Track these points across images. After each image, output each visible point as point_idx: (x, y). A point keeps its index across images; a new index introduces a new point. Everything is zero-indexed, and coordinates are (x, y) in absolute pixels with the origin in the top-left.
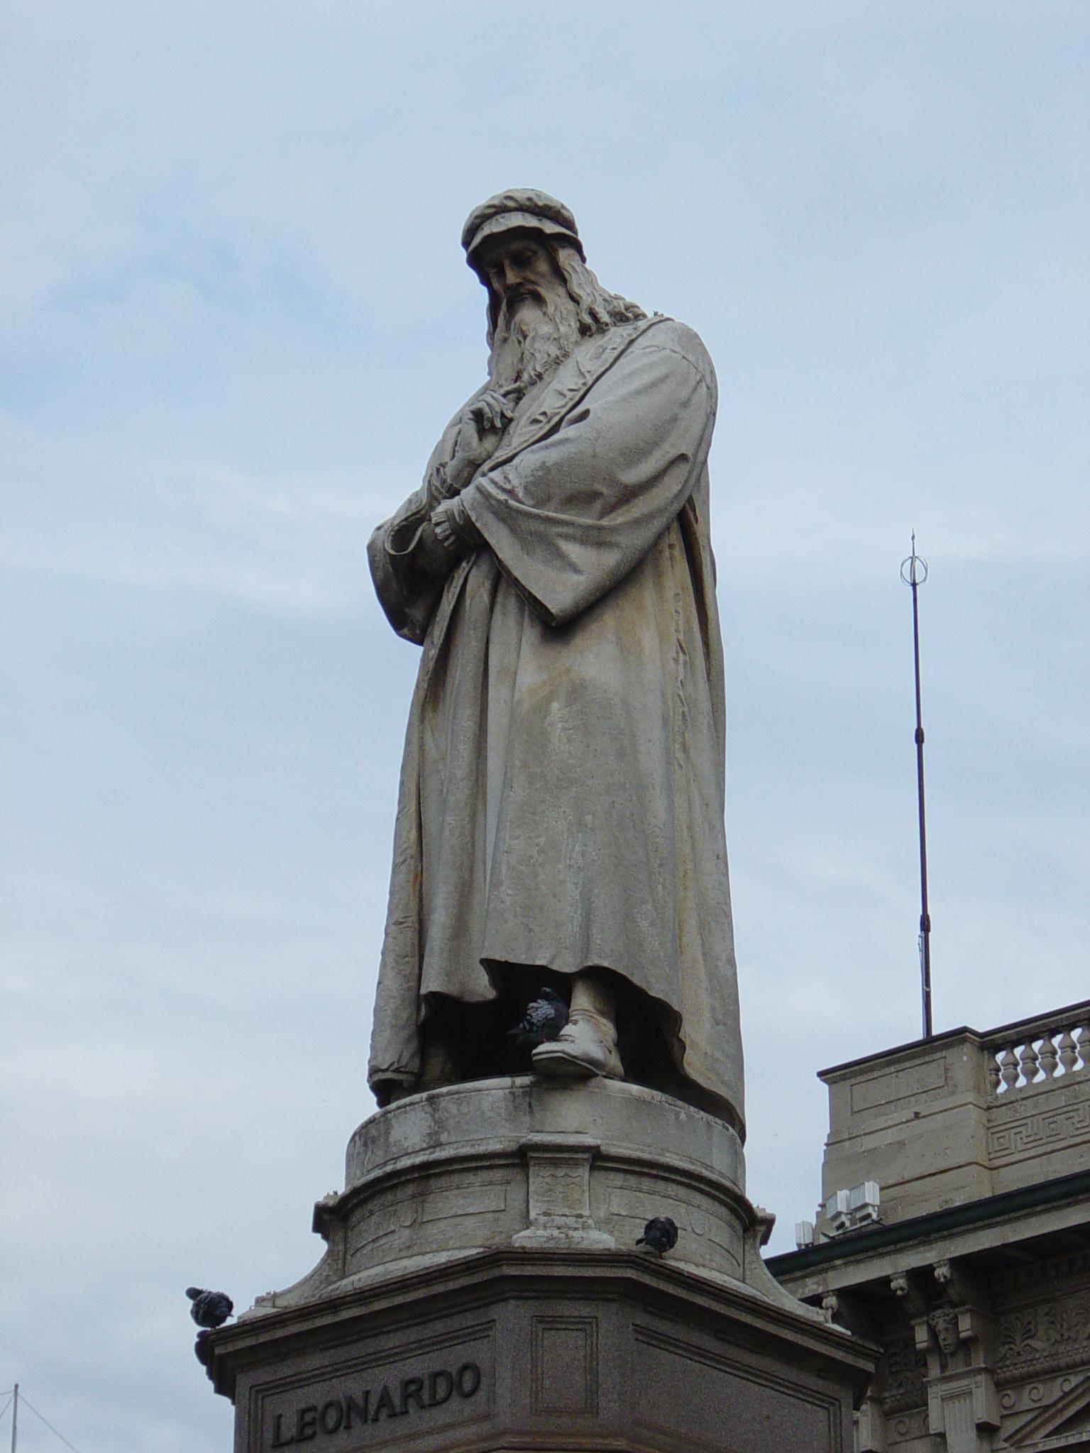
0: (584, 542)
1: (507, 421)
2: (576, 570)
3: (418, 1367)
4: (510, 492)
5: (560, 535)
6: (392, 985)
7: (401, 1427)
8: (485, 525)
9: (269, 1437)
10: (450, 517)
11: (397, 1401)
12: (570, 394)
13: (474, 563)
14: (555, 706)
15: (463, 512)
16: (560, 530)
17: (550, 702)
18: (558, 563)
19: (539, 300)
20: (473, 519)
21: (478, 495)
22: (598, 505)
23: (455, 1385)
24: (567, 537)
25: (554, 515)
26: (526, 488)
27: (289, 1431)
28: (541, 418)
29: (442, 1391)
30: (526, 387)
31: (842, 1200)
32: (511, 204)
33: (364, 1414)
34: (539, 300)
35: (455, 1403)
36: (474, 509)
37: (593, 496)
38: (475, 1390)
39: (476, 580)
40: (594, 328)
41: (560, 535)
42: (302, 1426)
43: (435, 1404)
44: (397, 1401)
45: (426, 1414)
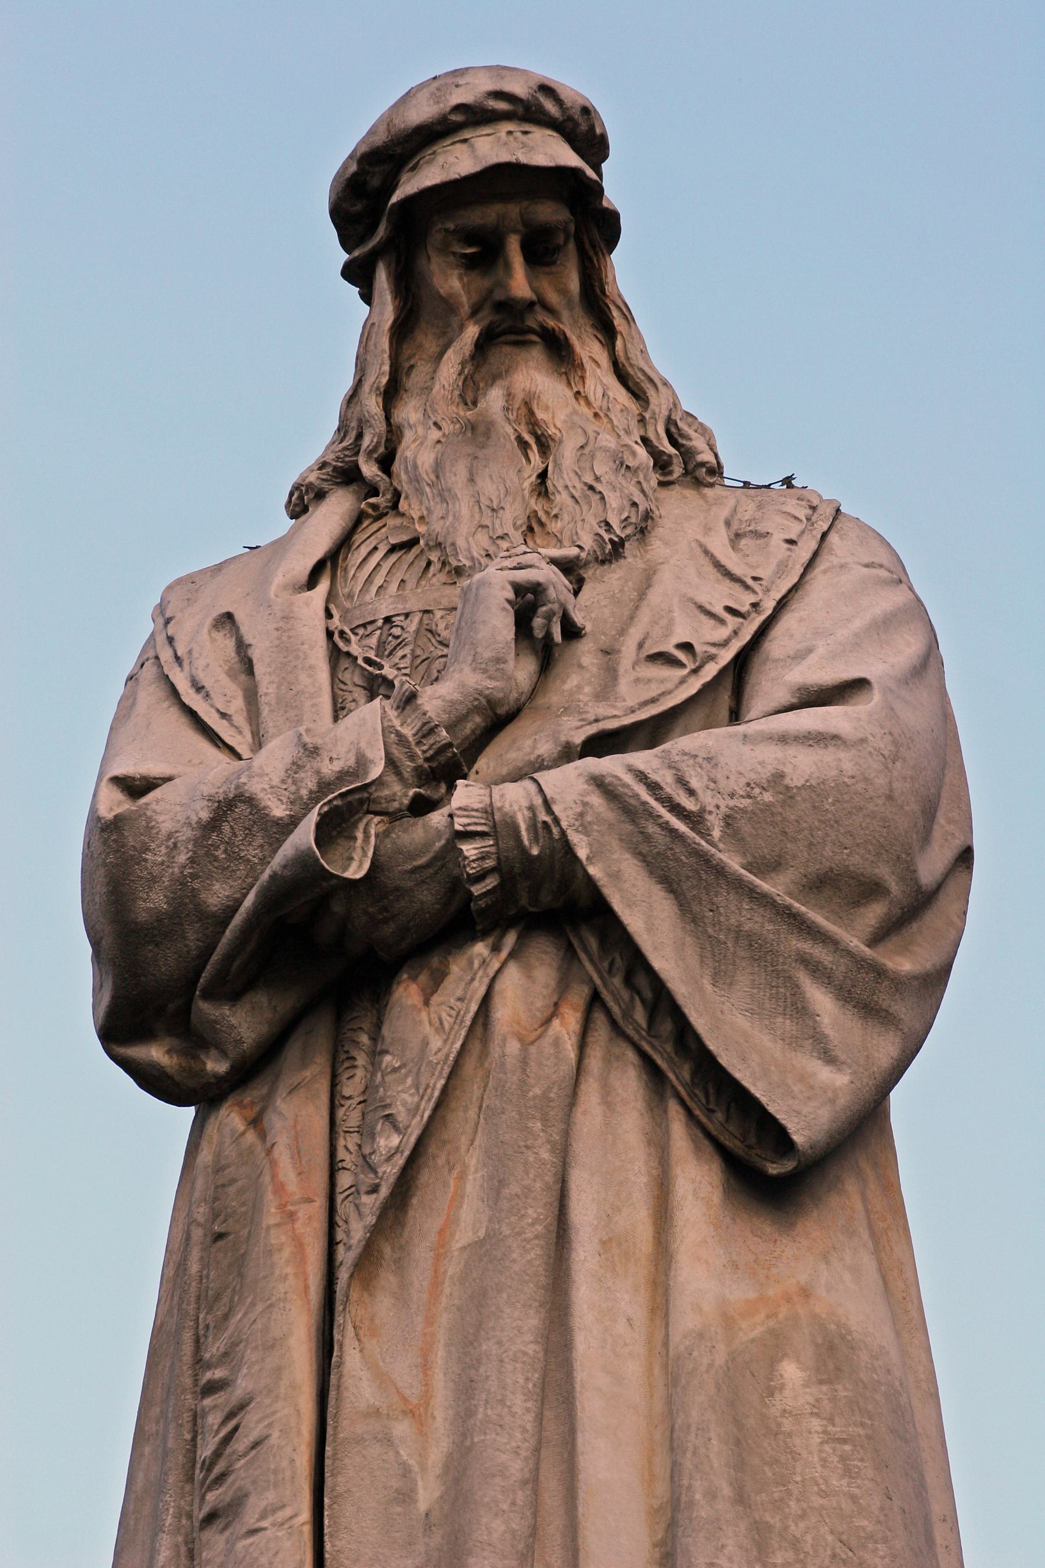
0: (844, 995)
2: (829, 1058)
4: (695, 820)
5: (804, 960)
8: (615, 876)
10: (497, 827)
12: (732, 621)
13: (513, 955)
14: (791, 1371)
15: (547, 828)
16: (806, 946)
17: (773, 1363)
18: (786, 1025)
19: (559, 352)
20: (582, 853)
21: (596, 800)
22: (874, 913)
24: (815, 969)
25: (803, 909)
26: (728, 821)
28: (681, 656)
30: (587, 564)
32: (550, 107)
36: (585, 829)
37: (870, 890)
40: (677, 470)
41: (804, 960)
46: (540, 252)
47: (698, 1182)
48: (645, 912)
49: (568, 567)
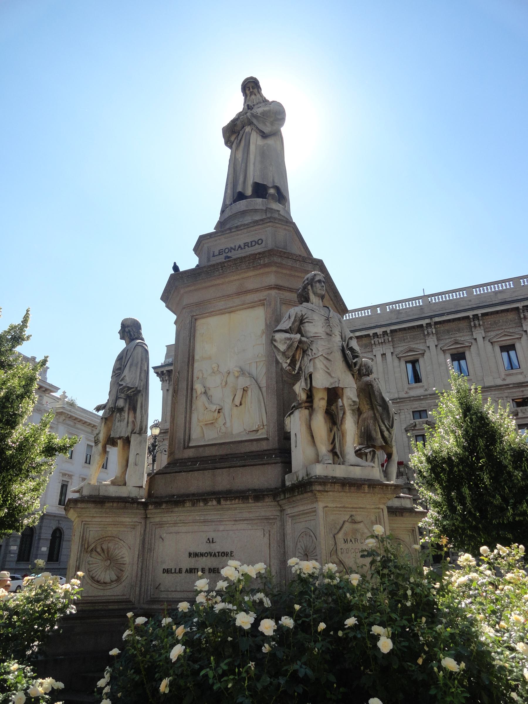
1: (253, 108)
3: (249, 240)
6: (229, 191)
7: (243, 251)
9: (212, 255)
11: (243, 247)
19: (255, 94)
23: (257, 243)
27: (217, 253)
29: (253, 243)
31: (168, 360)
33: (234, 250)
34: (255, 94)
35: (257, 245)
38: (262, 243)
39: (248, 129)
42: (219, 252)
43: (252, 246)
44: (243, 247)
45: (250, 248)
46: (253, 88)
47: (259, 138)
48: (255, 121)
49: (254, 105)
